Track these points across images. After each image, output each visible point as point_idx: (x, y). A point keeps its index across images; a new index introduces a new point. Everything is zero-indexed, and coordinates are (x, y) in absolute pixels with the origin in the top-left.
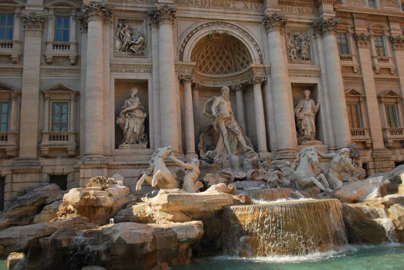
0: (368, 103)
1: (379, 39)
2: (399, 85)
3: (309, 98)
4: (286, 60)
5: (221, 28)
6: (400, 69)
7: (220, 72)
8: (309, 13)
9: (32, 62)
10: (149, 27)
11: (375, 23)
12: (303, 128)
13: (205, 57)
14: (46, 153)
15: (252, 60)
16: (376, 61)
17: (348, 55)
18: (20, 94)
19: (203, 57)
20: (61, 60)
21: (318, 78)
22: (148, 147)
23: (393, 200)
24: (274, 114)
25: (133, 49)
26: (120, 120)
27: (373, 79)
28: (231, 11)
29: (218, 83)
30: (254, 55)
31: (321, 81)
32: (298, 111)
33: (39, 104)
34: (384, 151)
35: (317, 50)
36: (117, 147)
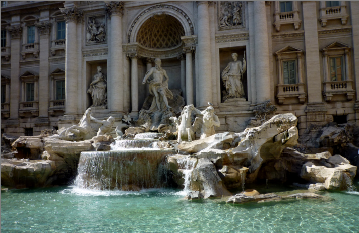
0: (308, 58)
2: (352, 34)
3: (238, 60)
5: (159, 10)
6: (353, 17)
9: (44, 56)
12: (227, 87)
13: (158, 36)
14: (52, 114)
15: (184, 33)
16: (323, 13)
17: (289, 12)
18: (39, 77)
19: (155, 35)
20: (61, 52)
21: (246, 41)
23: (206, 154)
24: (198, 78)
25: (98, 38)
26: (89, 91)
27: (316, 33)
29: (169, 55)
30: (186, 28)
31: (249, 44)
32: (225, 73)
33: (49, 83)
34: (322, 105)
35: (248, 14)
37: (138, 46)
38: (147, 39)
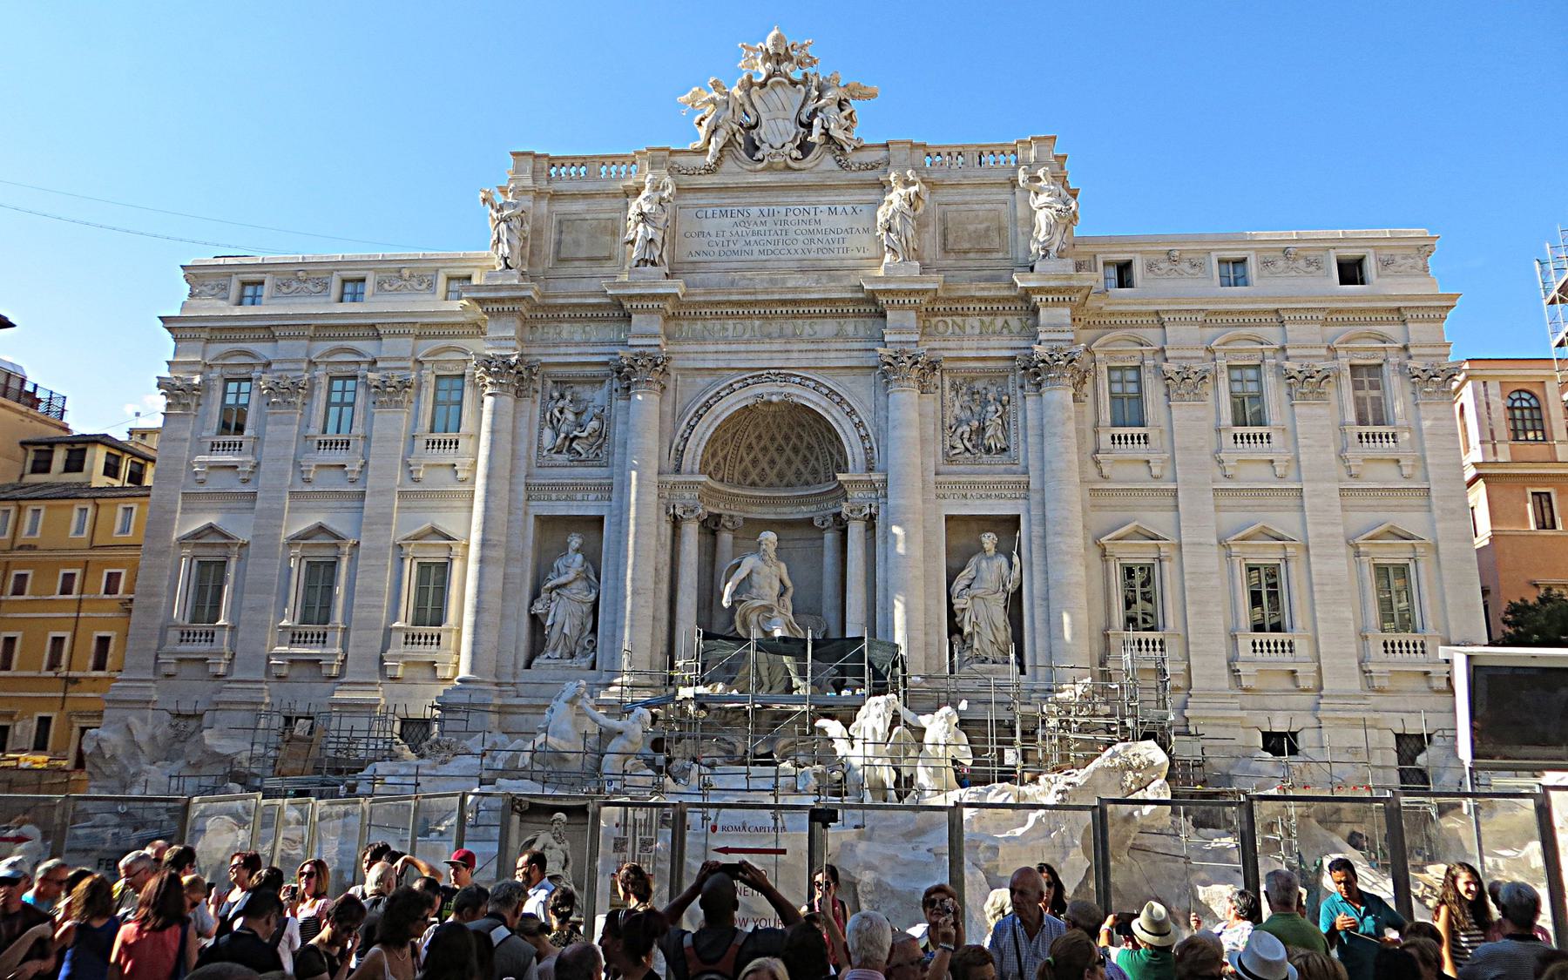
1: (1251, 374)
4: (934, 459)
7: (793, 479)
8: (1010, 332)
10: (615, 395)
11: (1234, 332)
12: (967, 629)
13: (757, 449)
16: (1228, 439)
19: (750, 447)
22: (593, 667)
26: (539, 608)
28: (804, 346)
30: (854, 449)
32: (958, 588)
36: (528, 666)
37: (705, 485)
38: (725, 459)
